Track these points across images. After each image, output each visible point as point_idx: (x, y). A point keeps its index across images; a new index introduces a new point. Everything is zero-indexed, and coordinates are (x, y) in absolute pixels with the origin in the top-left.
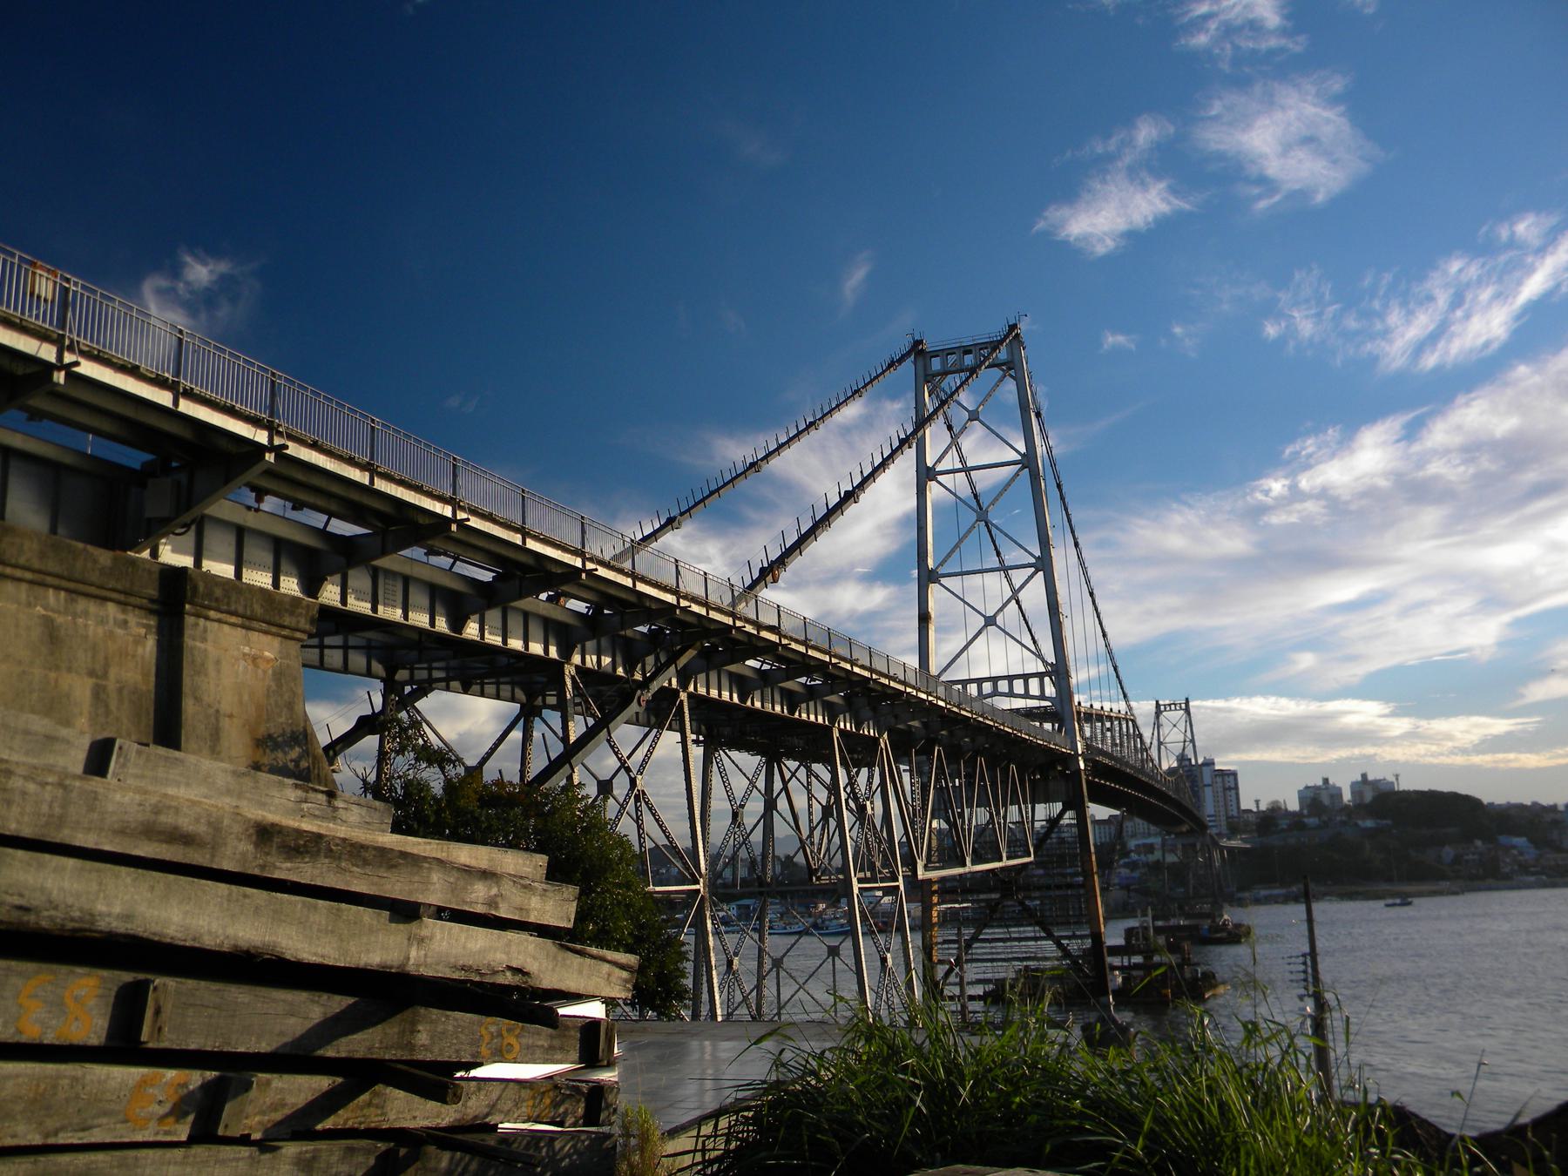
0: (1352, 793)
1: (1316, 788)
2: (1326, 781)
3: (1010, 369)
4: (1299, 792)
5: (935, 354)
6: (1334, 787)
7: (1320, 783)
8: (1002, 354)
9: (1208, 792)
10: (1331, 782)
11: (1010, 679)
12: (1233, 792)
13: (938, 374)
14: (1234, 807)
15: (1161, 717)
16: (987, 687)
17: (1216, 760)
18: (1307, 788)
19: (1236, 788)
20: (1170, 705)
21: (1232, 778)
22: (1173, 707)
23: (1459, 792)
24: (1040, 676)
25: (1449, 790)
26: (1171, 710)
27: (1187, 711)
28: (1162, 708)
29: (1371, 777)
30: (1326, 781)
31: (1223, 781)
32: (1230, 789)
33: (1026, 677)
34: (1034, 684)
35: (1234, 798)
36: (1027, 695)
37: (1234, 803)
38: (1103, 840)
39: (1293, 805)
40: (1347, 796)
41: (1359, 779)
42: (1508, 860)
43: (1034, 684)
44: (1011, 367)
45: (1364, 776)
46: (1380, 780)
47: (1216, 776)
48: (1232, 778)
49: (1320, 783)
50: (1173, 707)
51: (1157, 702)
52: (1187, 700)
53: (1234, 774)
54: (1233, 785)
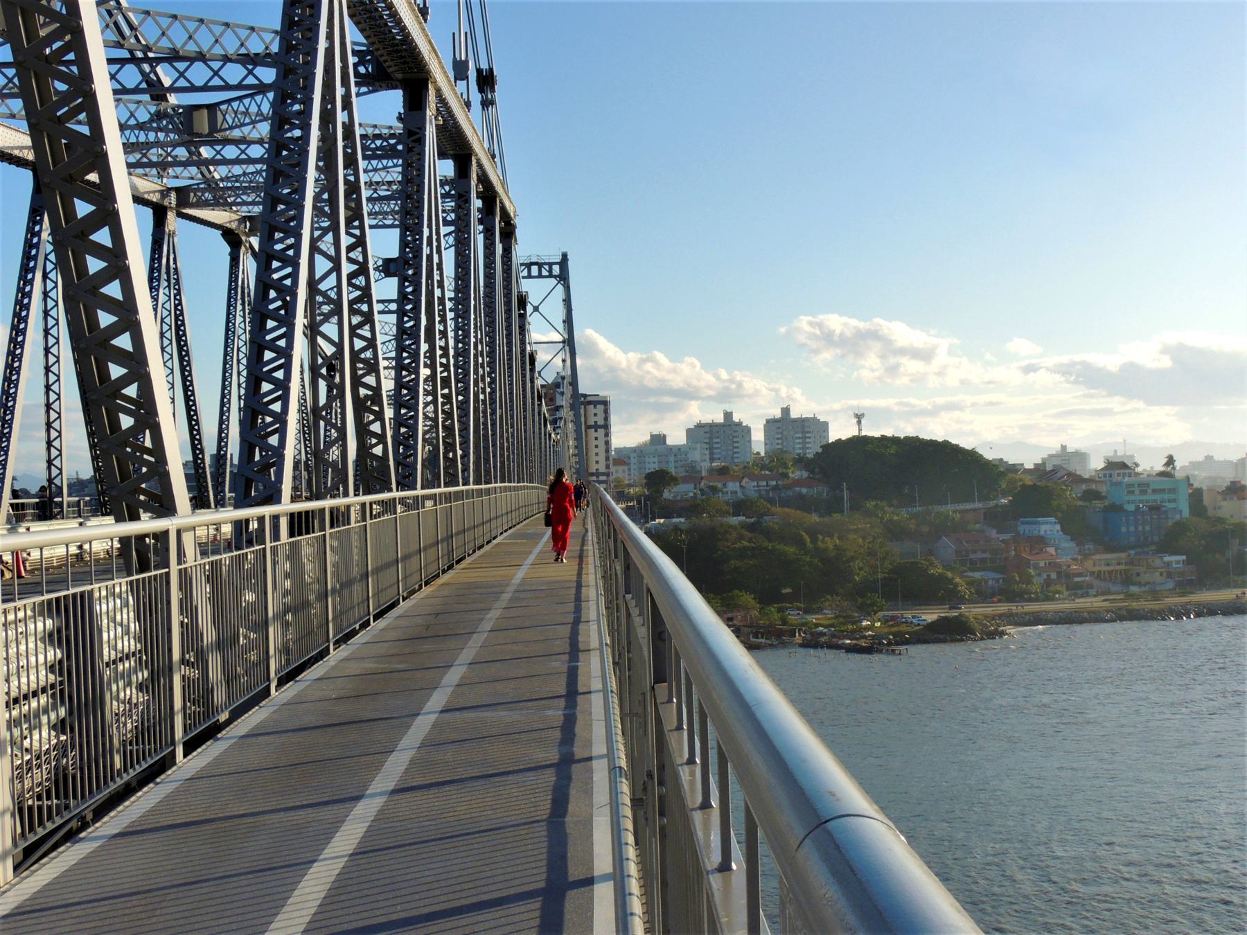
1: (712, 426)
2: (728, 415)
6: (740, 424)
7: (719, 418)
12: (601, 431)
14: (602, 458)
19: (606, 427)
22: (535, 270)
26: (530, 276)
27: (563, 278)
29: (794, 414)
30: (728, 415)
32: (596, 427)
35: (601, 443)
37: (602, 447)
42: (1042, 564)
45: (786, 411)
46: (807, 419)
48: (601, 408)
50: (535, 270)
52: (565, 256)
54: (601, 422)
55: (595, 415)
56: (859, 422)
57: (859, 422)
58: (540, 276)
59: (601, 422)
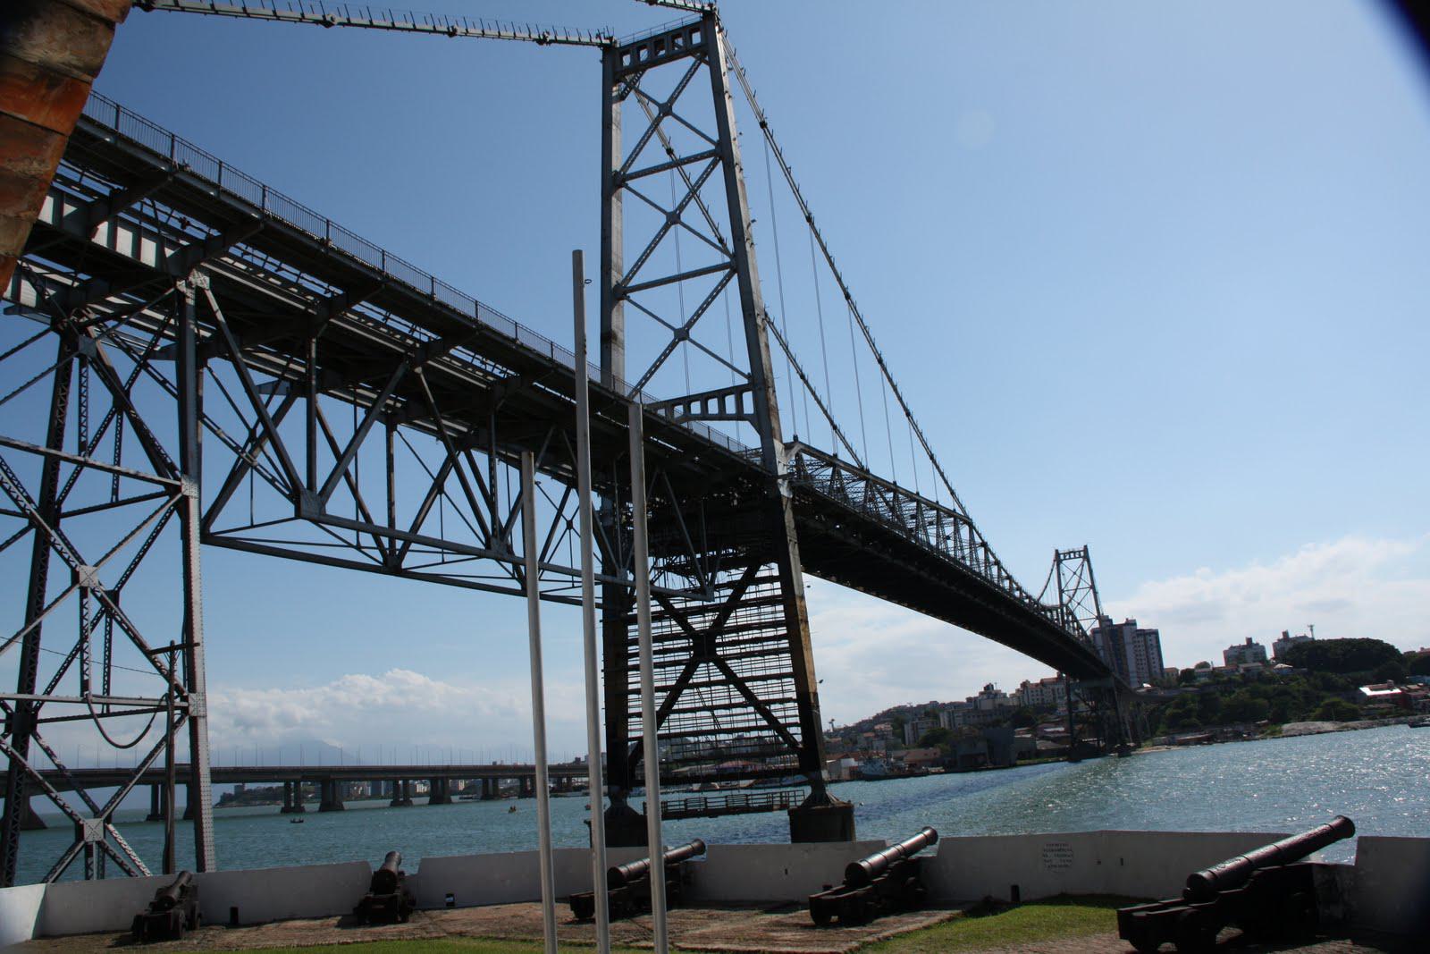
0: (1276, 651)
1: (1241, 648)
2: (1249, 640)
3: (705, 55)
4: (1225, 652)
5: (625, 50)
6: (1257, 644)
7: (1245, 643)
8: (697, 38)
9: (1130, 650)
10: (1254, 642)
11: (704, 398)
13: (628, 70)
14: (1157, 665)
15: (1061, 565)
16: (679, 409)
17: (1138, 624)
18: (1232, 648)
20: (1069, 553)
22: (1072, 555)
23: (1370, 638)
24: (738, 391)
25: (1360, 637)
26: (1070, 558)
27: (1086, 558)
28: (1062, 557)
29: (1291, 635)
30: (1249, 640)
31: (1145, 640)
33: (721, 395)
34: (730, 401)
35: (1156, 655)
36: (722, 416)
37: (1157, 661)
38: (1036, 702)
39: (1219, 662)
40: (1270, 654)
41: (1281, 637)
43: (730, 401)
44: (706, 53)
45: (1285, 634)
47: (1138, 635)
48: (1153, 637)
49: (1245, 643)
50: (1072, 555)
51: (1057, 551)
52: (1086, 547)
53: (1155, 633)
56: (1312, 630)
57: (1312, 630)
58: (1075, 558)
59: (1154, 642)
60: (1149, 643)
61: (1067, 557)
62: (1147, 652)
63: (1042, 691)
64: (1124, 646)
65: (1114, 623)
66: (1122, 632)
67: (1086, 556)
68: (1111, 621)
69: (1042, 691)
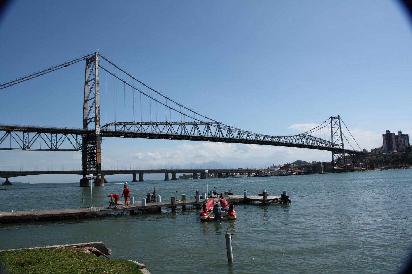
14: (407, 144)
20: (335, 117)
21: (406, 136)
22: (335, 118)
35: (407, 142)
47: (401, 136)
48: (406, 136)
52: (339, 116)
53: (407, 135)
55: (405, 137)
59: (407, 138)
60: (405, 138)
61: (334, 118)
62: (404, 141)
63: (376, 151)
64: (392, 139)
65: (390, 132)
66: (392, 135)
67: (338, 118)
68: (389, 132)
69: (376, 151)
